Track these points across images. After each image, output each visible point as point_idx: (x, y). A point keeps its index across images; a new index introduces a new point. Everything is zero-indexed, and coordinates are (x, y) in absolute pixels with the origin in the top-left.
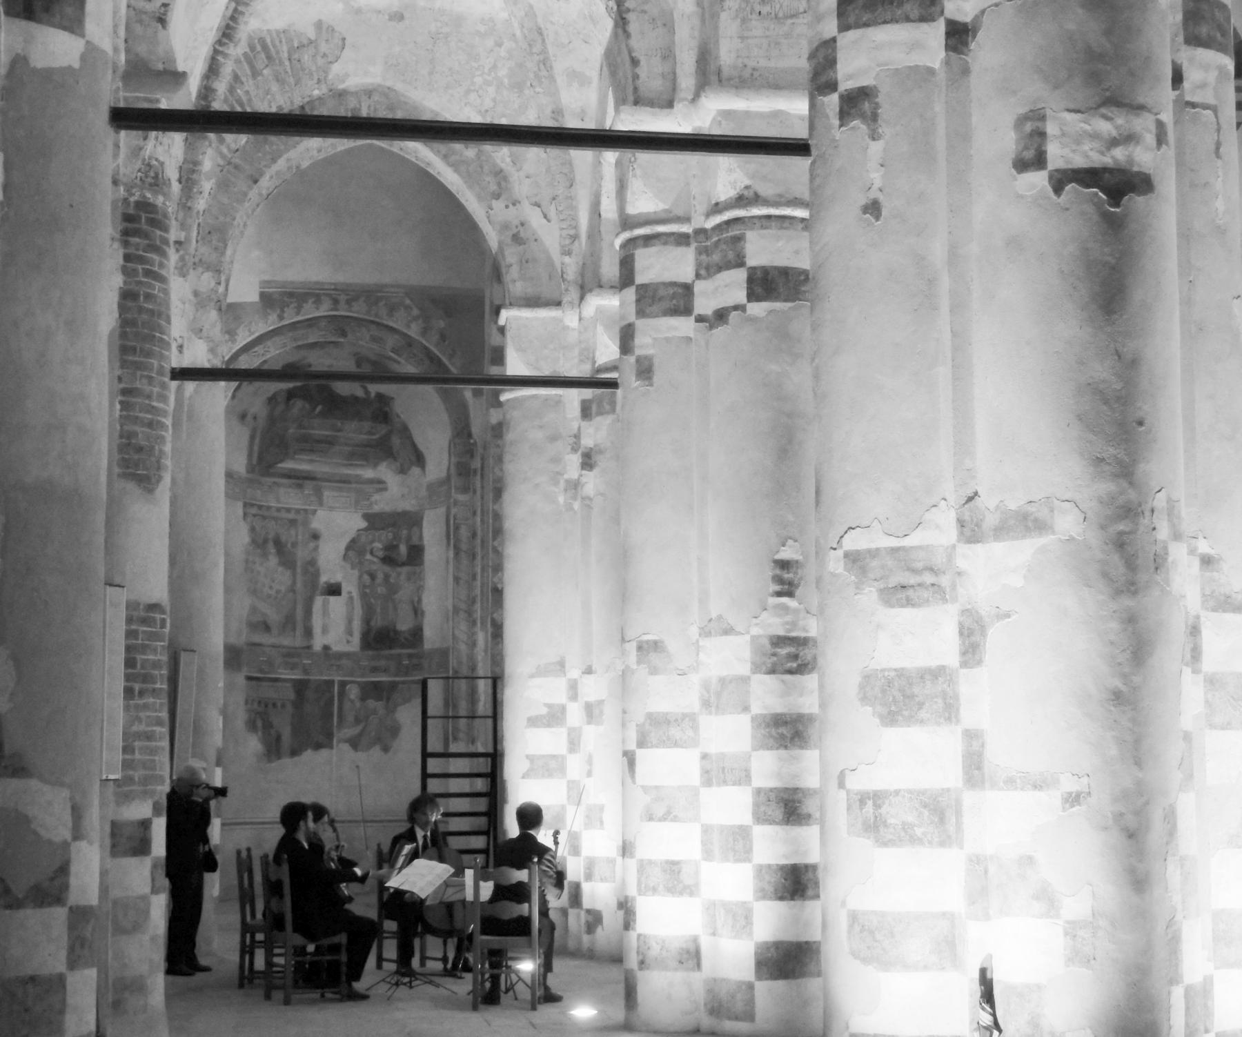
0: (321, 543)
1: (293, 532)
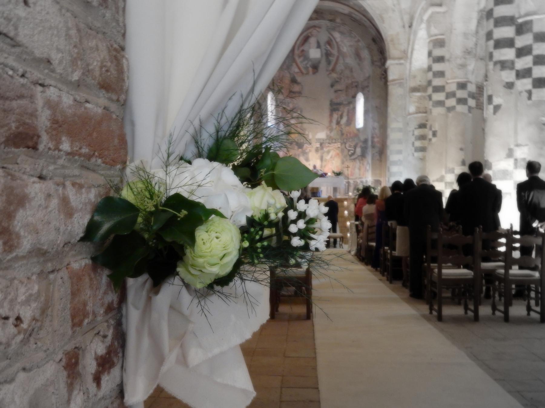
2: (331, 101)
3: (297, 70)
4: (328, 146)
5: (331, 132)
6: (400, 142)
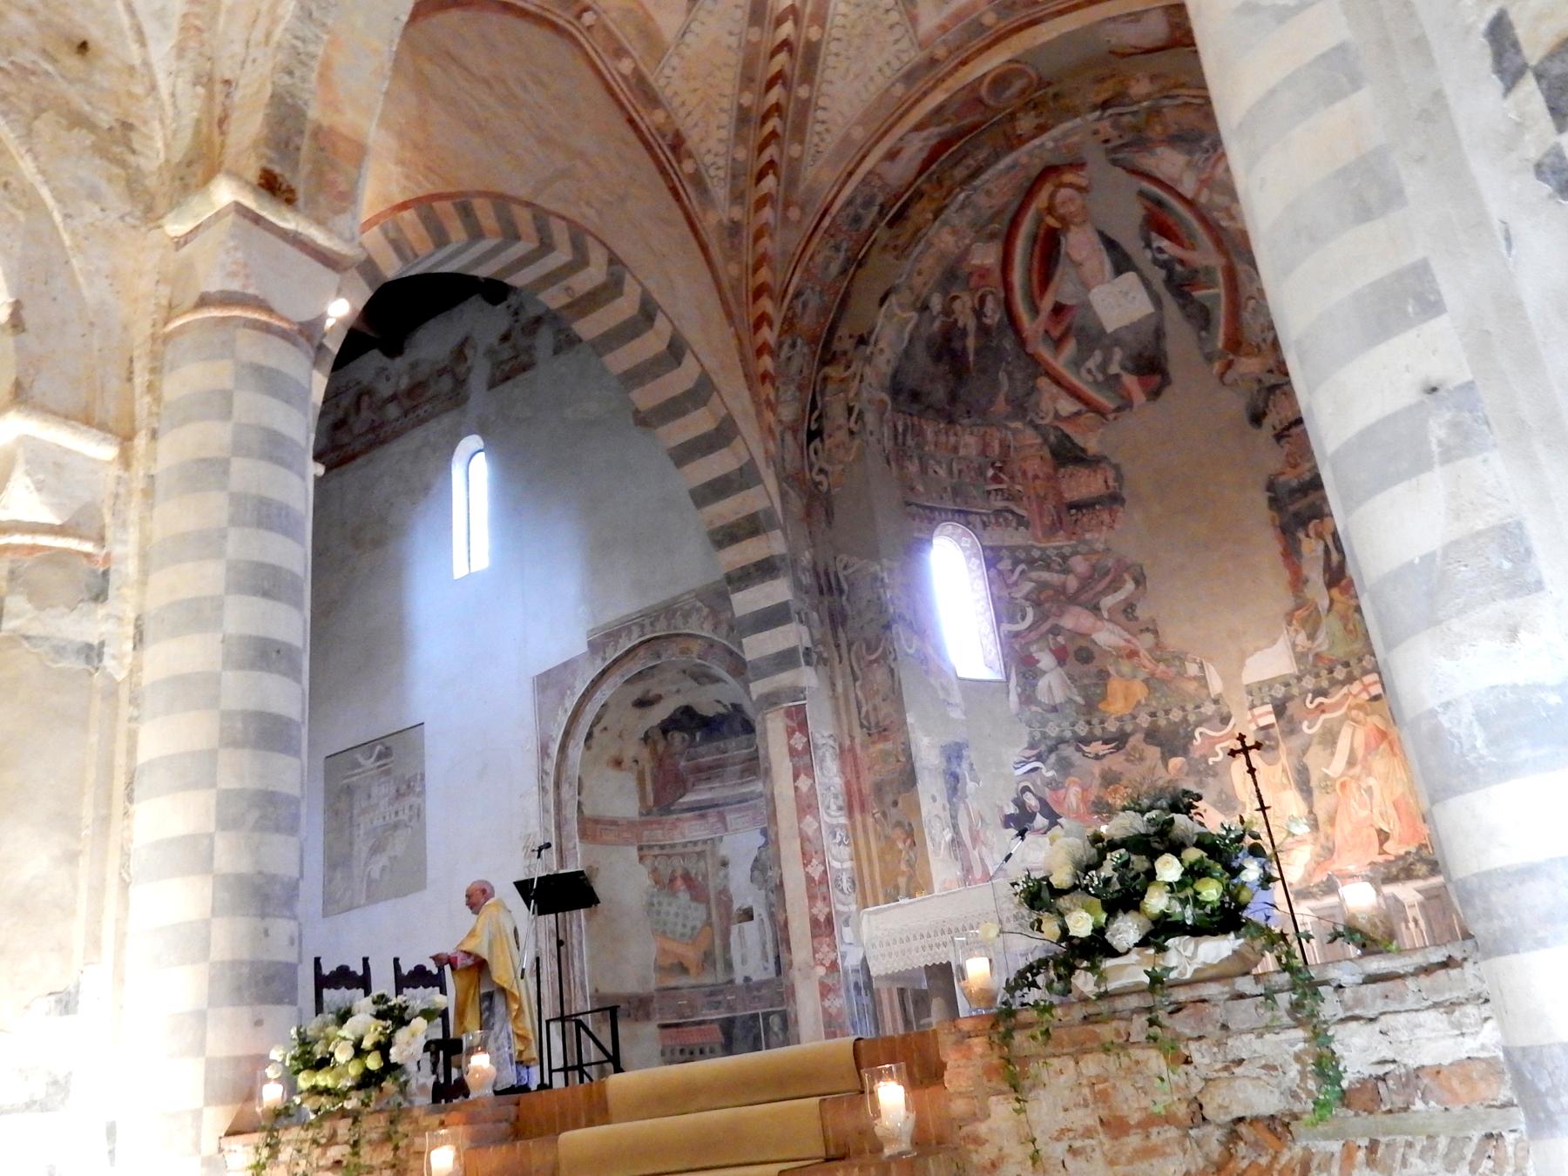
0: (731, 870)
1: (702, 864)
2: (1271, 486)
3: (1067, 406)
4: (1321, 709)
5: (1311, 637)
6: (1367, 190)
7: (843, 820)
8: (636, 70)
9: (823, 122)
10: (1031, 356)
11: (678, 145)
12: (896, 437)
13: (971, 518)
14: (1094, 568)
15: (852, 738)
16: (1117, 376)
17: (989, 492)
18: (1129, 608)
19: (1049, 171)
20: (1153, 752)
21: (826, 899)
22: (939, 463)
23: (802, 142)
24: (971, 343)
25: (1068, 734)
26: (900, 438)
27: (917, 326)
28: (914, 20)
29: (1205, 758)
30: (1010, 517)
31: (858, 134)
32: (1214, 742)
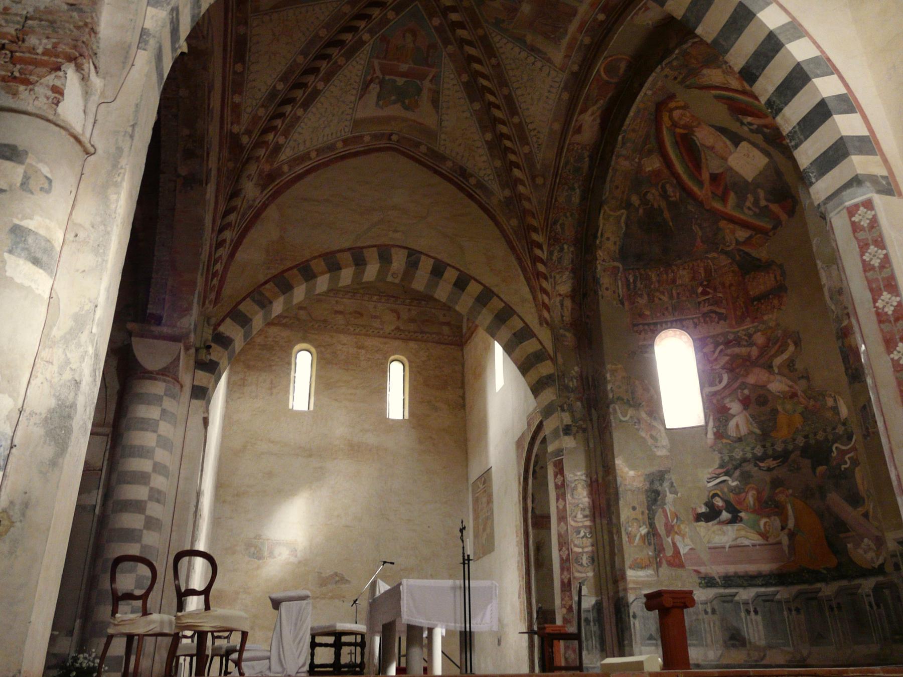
7: (588, 523)
8: (428, 148)
9: (535, 129)
10: (707, 210)
11: (463, 173)
12: (628, 285)
13: (684, 323)
14: (769, 339)
15: (597, 473)
16: (766, 207)
17: (699, 303)
18: (790, 364)
19: (660, 107)
20: (806, 463)
21: (568, 569)
22: (663, 293)
23: (528, 144)
24: (667, 215)
25: (749, 456)
26: (632, 287)
27: (628, 217)
28: (549, 60)
29: (839, 466)
30: (714, 316)
31: (557, 126)
32: (843, 453)
